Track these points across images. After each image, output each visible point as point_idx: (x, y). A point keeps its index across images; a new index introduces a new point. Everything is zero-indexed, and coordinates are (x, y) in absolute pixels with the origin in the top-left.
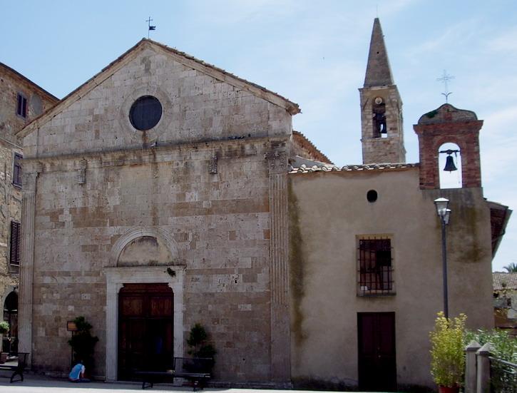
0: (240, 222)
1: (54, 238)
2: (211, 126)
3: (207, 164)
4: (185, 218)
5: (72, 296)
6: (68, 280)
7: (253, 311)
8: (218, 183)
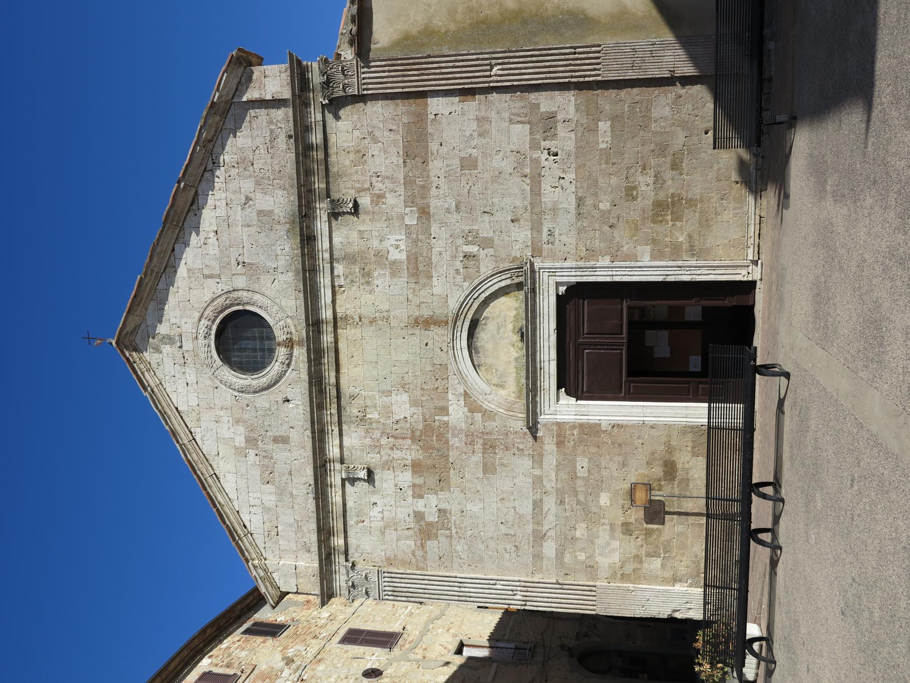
0: (444, 149)
1: (469, 533)
2: (271, 212)
5: (581, 497)
6: (550, 503)
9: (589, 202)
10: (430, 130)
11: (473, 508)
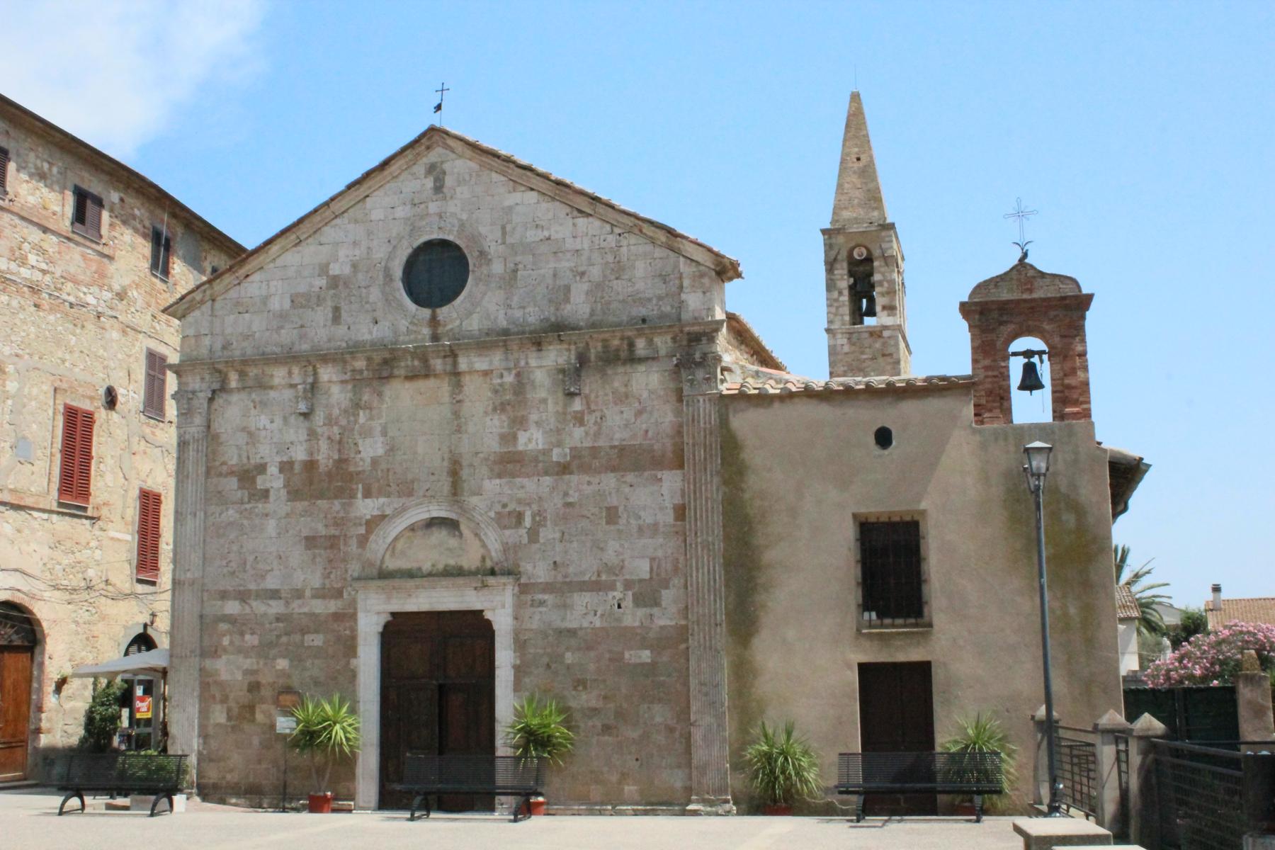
0: (627, 490)
1: (245, 522)
3: (561, 376)
4: (518, 480)
5: (284, 639)
6: (276, 607)
7: (653, 665)
8: (582, 413)
9: (573, 642)
10: (646, 474)
11: (271, 526)
